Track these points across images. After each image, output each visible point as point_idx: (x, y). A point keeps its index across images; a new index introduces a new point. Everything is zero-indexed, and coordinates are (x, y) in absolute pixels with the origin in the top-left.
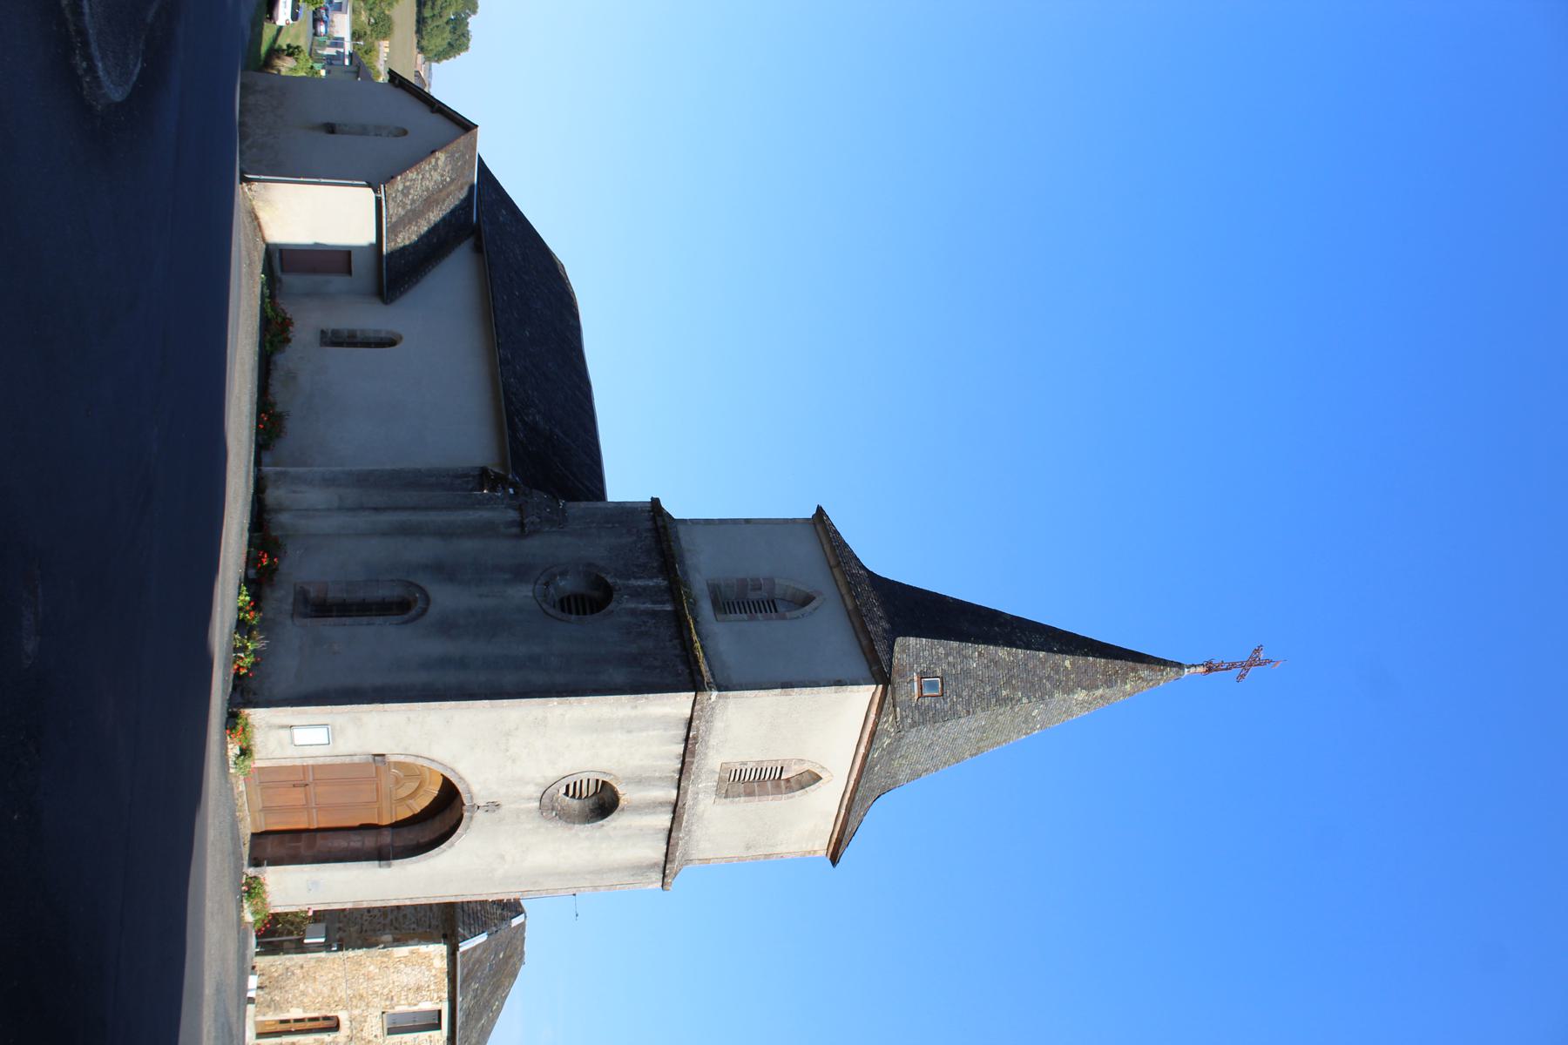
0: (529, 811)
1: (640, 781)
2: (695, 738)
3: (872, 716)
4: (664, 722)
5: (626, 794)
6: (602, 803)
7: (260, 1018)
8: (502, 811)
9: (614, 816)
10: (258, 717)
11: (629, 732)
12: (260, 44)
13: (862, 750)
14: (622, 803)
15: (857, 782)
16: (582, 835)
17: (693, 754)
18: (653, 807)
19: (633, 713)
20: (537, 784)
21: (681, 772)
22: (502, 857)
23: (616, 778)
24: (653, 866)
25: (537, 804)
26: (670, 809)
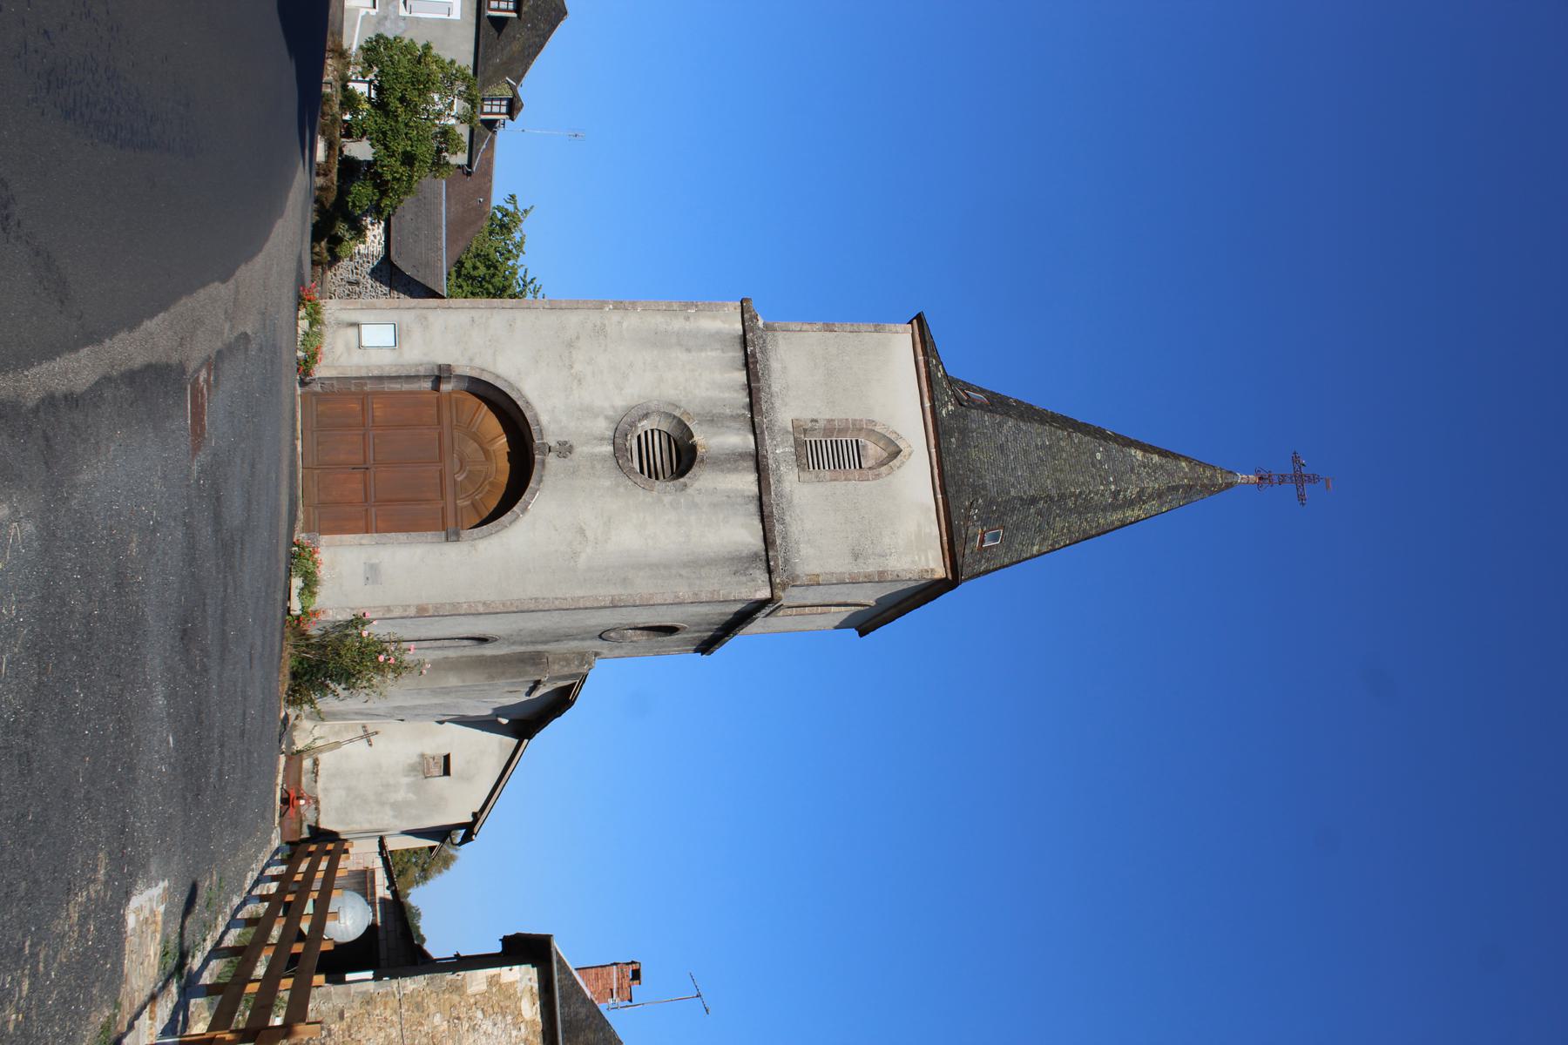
0: (604, 459)
1: (713, 420)
2: (754, 355)
3: (921, 358)
4: (716, 338)
5: (705, 439)
6: (682, 457)
7: (320, 408)
8: (575, 456)
9: (695, 469)
10: (370, 158)
11: (688, 350)
12: (415, 852)
13: (927, 404)
14: (700, 451)
15: (937, 446)
16: (667, 499)
17: (758, 402)
18: (728, 461)
19: (688, 326)
20: (607, 418)
21: (751, 406)
22: (582, 531)
23: (686, 413)
24: (755, 556)
25: (611, 448)
26: (751, 464)
